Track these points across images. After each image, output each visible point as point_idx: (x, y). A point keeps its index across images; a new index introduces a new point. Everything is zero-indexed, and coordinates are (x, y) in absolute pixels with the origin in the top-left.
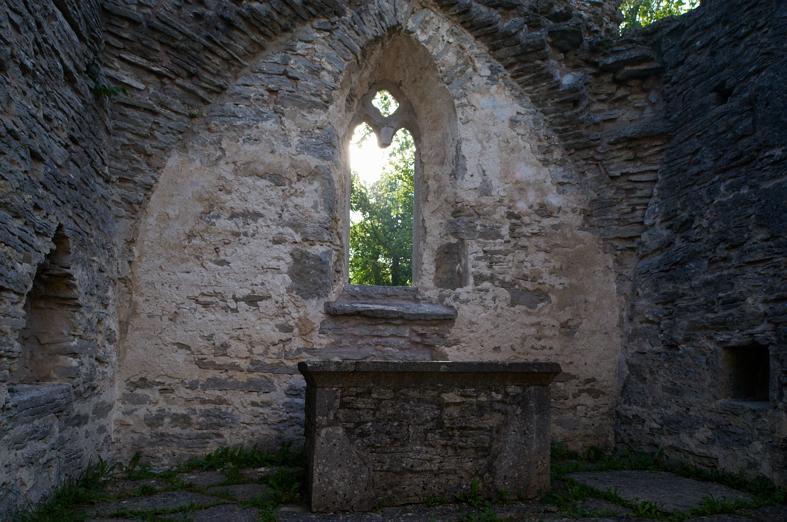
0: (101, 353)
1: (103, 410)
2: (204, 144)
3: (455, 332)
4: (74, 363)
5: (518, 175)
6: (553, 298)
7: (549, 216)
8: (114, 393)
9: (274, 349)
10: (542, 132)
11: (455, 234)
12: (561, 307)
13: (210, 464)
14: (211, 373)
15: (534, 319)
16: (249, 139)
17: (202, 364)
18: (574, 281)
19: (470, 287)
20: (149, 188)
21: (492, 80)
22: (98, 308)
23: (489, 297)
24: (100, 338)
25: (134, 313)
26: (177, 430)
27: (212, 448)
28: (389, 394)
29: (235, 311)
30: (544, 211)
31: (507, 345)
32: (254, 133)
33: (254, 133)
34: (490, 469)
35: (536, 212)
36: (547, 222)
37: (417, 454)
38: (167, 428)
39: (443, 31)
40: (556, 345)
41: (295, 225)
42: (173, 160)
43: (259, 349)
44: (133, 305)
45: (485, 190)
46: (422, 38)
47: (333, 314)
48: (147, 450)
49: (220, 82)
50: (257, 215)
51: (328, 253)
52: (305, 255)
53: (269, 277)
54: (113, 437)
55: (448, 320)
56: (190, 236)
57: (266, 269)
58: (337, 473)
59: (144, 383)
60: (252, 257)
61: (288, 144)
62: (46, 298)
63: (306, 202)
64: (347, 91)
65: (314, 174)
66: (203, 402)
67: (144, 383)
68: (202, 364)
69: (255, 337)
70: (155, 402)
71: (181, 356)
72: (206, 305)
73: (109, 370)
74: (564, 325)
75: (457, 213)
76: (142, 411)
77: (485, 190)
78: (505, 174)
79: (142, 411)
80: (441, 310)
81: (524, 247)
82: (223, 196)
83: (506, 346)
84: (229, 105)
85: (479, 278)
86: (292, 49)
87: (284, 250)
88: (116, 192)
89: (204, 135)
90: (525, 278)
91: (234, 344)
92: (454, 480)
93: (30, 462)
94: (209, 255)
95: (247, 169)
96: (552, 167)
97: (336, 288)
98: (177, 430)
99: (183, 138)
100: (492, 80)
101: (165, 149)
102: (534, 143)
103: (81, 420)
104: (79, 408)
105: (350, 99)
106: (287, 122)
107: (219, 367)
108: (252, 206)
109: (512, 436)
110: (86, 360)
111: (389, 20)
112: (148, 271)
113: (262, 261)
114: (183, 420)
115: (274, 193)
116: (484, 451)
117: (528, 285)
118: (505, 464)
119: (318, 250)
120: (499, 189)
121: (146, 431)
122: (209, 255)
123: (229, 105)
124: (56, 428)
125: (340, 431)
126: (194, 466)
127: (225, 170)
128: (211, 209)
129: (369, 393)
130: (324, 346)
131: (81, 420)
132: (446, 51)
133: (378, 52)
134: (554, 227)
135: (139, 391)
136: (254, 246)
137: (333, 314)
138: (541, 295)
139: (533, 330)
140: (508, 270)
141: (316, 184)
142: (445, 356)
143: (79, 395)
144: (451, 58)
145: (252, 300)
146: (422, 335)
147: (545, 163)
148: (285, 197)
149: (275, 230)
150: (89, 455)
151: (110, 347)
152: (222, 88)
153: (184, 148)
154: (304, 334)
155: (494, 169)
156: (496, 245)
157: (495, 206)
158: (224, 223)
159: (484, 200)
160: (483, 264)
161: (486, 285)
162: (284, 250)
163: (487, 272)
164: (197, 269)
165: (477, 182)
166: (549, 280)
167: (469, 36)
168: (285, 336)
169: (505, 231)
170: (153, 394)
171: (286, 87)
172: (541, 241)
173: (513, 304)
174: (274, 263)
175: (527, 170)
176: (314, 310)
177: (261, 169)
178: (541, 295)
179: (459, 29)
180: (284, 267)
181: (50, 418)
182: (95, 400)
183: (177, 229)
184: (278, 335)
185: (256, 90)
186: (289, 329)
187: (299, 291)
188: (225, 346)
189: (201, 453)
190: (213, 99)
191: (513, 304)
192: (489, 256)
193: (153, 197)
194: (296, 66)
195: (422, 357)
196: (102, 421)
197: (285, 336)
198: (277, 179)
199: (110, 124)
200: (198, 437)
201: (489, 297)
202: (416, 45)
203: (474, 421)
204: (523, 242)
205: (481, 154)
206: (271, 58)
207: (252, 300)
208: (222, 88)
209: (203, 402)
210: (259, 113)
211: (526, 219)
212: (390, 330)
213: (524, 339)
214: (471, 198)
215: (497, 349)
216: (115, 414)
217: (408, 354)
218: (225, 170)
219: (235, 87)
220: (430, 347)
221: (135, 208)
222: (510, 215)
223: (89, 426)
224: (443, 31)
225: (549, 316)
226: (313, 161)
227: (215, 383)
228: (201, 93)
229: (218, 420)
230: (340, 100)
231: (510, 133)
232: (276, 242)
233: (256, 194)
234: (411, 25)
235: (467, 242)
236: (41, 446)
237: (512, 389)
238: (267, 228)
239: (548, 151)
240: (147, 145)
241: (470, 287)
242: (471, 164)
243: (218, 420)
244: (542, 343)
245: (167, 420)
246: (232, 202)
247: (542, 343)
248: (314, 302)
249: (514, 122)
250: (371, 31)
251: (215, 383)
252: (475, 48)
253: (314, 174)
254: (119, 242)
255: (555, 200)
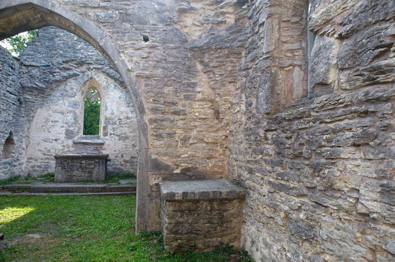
0: (21, 152)
1: (21, 164)
2: (46, 106)
3: (104, 147)
4: (14, 155)
5: (121, 110)
6: (130, 139)
7: (129, 119)
8: (24, 160)
9: (61, 151)
10: (128, 99)
11: (105, 124)
12: (132, 140)
13: (45, 176)
14: (46, 156)
15: (125, 144)
16: (56, 105)
17: (44, 154)
18: (136, 134)
19: (109, 136)
20: (33, 116)
21: (115, 88)
22: (20, 143)
23: (113, 139)
24: (20, 149)
25: (29, 143)
26: (38, 169)
27: (46, 173)
28: (70, 161)
29: (52, 142)
30: (128, 118)
31: (118, 150)
32: (57, 104)
33: (57, 104)
34: (91, 176)
35: (126, 118)
36: (128, 120)
37: (76, 173)
38: (36, 168)
39: (103, 78)
40: (131, 150)
41: (66, 123)
42: (39, 110)
43: (57, 151)
44: (29, 141)
45: (113, 114)
46: (97, 80)
47: (74, 143)
48: (31, 173)
49: (50, 93)
50: (57, 121)
51: (75, 129)
52: (68, 130)
53: (60, 135)
54: (24, 170)
55: (102, 144)
56: (42, 126)
57: (59, 133)
58: (59, 176)
59: (31, 158)
60: (56, 131)
61: (65, 105)
62: (9, 143)
63: (69, 118)
64: (81, 92)
65: (71, 112)
66: (44, 163)
67: (31, 158)
68: (44, 154)
69: (56, 148)
70: (33, 163)
71: (40, 152)
72: (45, 141)
73: (23, 156)
74: (133, 145)
75: (106, 119)
76: (30, 165)
77: (113, 114)
78: (118, 110)
79: (30, 165)
80: (102, 142)
81: (122, 127)
82: (50, 118)
83: (117, 150)
84: (52, 98)
85: (111, 134)
86: (67, 85)
87: (64, 129)
88: (26, 118)
89: (46, 105)
90: (123, 134)
91: (51, 150)
92: (83, 178)
93: (3, 172)
94: (46, 131)
95: (55, 112)
96: (130, 108)
97: (77, 136)
98: (38, 169)
99: (42, 105)
100: (115, 88)
101: (37, 108)
102: (126, 102)
103: (15, 166)
104: (14, 163)
105: (83, 92)
106: (65, 100)
107: (48, 155)
108: (56, 120)
109: (96, 169)
110: (16, 154)
111: (90, 76)
112: (33, 134)
113: (58, 131)
114: (40, 167)
115: (62, 116)
116: (90, 172)
117: (124, 136)
118: (94, 175)
119: (71, 129)
120: (116, 113)
121: (31, 169)
122: (46, 131)
123: (52, 98)
124: (9, 167)
125: (60, 168)
126: (42, 176)
127: (51, 112)
128: (47, 121)
129: (66, 161)
130: (72, 152)
131: (15, 166)
132: (103, 82)
133: (88, 82)
134: (130, 122)
135: (30, 160)
136: (56, 128)
137: (74, 143)
138: (127, 138)
139: (125, 146)
140: (118, 132)
141: (71, 114)
142: (102, 153)
143: (15, 161)
144: (105, 84)
145: (56, 140)
146: (96, 148)
147: (128, 106)
148: (64, 117)
149: (62, 125)
150: (17, 173)
151: (23, 151)
152: (51, 94)
153: (42, 107)
154: (68, 148)
155: (115, 109)
156: (116, 126)
157: (115, 117)
158: (50, 123)
159: (112, 116)
160: (112, 131)
161: (113, 136)
162: (64, 129)
163: (113, 133)
164: (44, 133)
165: (111, 112)
166: (129, 134)
167: (109, 78)
168: (63, 148)
169: (118, 123)
170: (33, 161)
171: (65, 93)
172: (127, 125)
173: (119, 140)
174: (61, 132)
175: (124, 108)
176: (70, 142)
177: (59, 111)
178: (127, 138)
179: (107, 77)
180: (63, 132)
181: (8, 165)
182: (19, 162)
183: (39, 125)
184: (62, 148)
185: (58, 94)
186: (65, 146)
187: (67, 138)
188: (49, 150)
189: (43, 174)
190: (49, 97)
191: (119, 140)
192: (114, 129)
193: (35, 118)
194: (68, 88)
195: (95, 153)
196: (21, 167)
197: (63, 148)
198: (62, 113)
199: (24, 106)
200: (43, 170)
201: (113, 139)
202: (96, 81)
203: (88, 166)
204: (122, 125)
205: (112, 105)
206: (62, 87)
207: (56, 140)
208: (51, 94)
209: (44, 163)
210: (59, 99)
211: (123, 120)
212: (89, 146)
213: (122, 148)
214: (109, 116)
215: (115, 151)
216: (24, 165)
217: (93, 152)
218: (51, 112)
219: (53, 94)
220: (99, 150)
221: (30, 121)
222: (119, 119)
223: (17, 167)
224: (103, 78)
225: (129, 143)
226: (71, 109)
227: (47, 158)
228: (45, 96)
229: (47, 167)
230: (79, 94)
231: (119, 100)
232: (62, 127)
233: (58, 117)
234: (95, 77)
235: (108, 126)
236: (5, 170)
237: (96, 160)
238: (60, 124)
239: (129, 104)
240: (33, 109)
241: (109, 136)
242: (109, 108)
243: (47, 167)
244: (127, 149)
245: (36, 167)
246: (52, 119)
247: (127, 149)
248: (70, 140)
249: (120, 98)
250: (86, 79)
251: (47, 158)
252: (111, 81)
253: (71, 112)
254: (26, 129)
255: (130, 115)
